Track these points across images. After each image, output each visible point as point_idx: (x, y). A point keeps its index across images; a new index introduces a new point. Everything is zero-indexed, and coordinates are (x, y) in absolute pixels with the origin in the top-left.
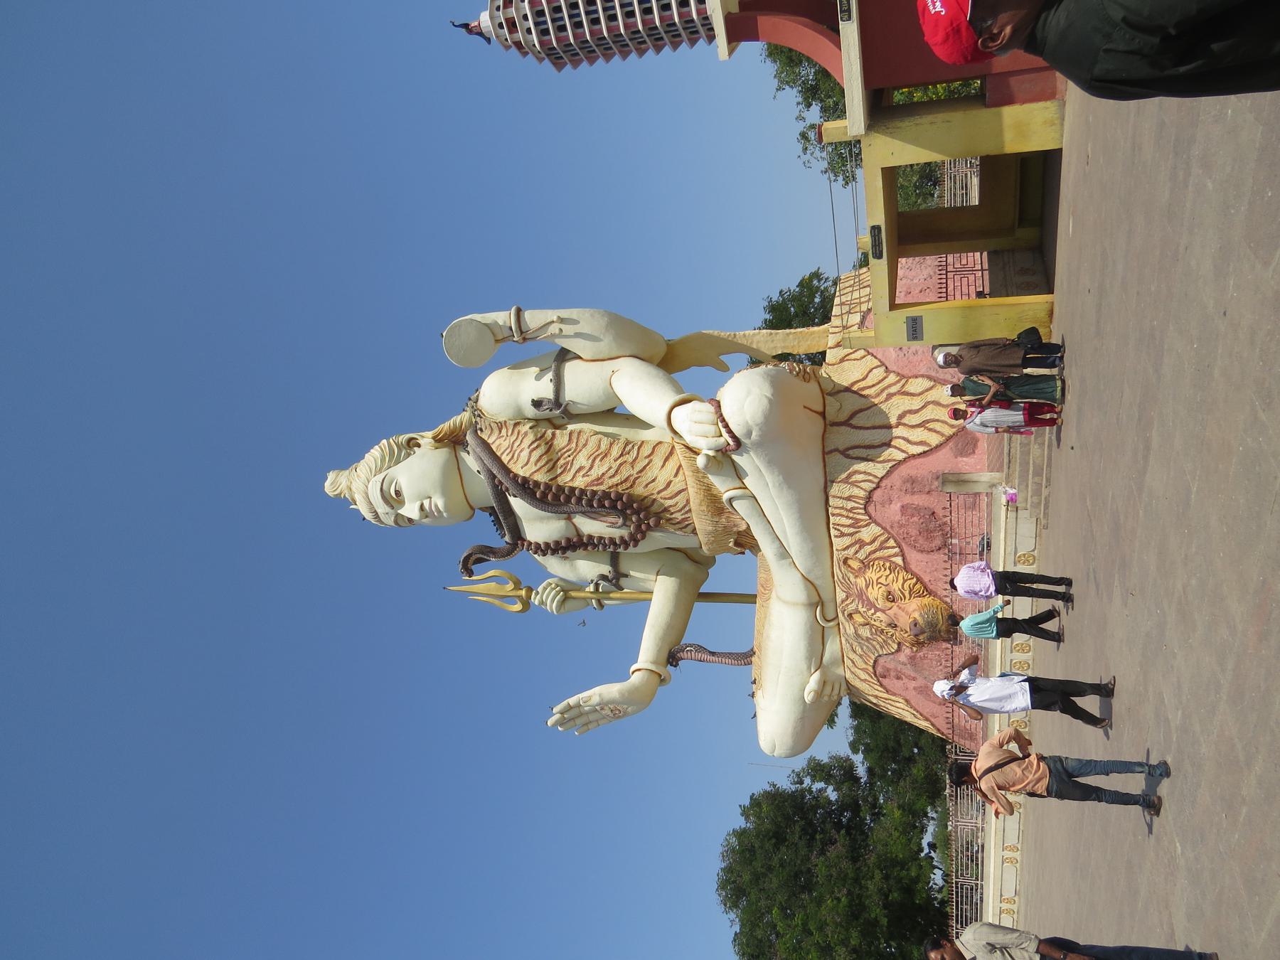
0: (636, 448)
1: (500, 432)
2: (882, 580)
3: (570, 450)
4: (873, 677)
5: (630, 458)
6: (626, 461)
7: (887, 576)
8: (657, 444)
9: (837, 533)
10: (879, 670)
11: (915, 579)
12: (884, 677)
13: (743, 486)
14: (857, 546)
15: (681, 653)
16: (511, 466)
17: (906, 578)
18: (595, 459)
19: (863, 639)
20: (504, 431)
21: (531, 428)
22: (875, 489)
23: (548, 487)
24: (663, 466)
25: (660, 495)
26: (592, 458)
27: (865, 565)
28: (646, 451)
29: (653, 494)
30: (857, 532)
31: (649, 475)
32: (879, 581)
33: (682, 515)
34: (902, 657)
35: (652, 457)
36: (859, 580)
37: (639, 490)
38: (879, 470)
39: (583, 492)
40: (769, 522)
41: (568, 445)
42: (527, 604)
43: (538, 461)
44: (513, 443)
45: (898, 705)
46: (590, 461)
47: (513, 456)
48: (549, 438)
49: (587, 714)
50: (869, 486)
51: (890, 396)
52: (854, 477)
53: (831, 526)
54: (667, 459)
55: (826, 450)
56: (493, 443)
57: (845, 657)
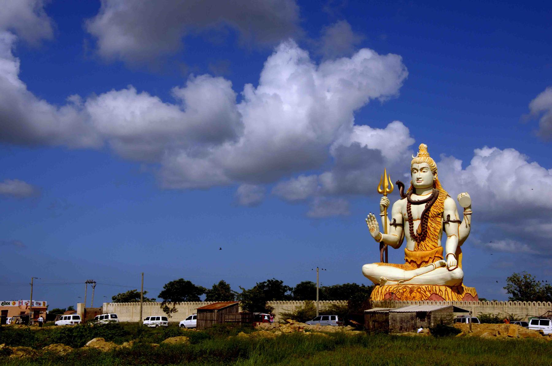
2: (417, 296)
5: (434, 237)
9: (426, 287)
12: (389, 294)
14: (424, 291)
16: (433, 206)
18: (434, 228)
20: (440, 204)
22: (439, 296)
23: (428, 216)
24: (433, 245)
25: (425, 244)
27: (420, 292)
28: (436, 241)
30: (427, 291)
31: (430, 241)
37: (427, 239)
38: (443, 297)
39: (427, 225)
41: (437, 221)
42: (382, 194)
45: (381, 297)
46: (434, 227)
50: (440, 294)
51: (458, 299)
54: (434, 246)
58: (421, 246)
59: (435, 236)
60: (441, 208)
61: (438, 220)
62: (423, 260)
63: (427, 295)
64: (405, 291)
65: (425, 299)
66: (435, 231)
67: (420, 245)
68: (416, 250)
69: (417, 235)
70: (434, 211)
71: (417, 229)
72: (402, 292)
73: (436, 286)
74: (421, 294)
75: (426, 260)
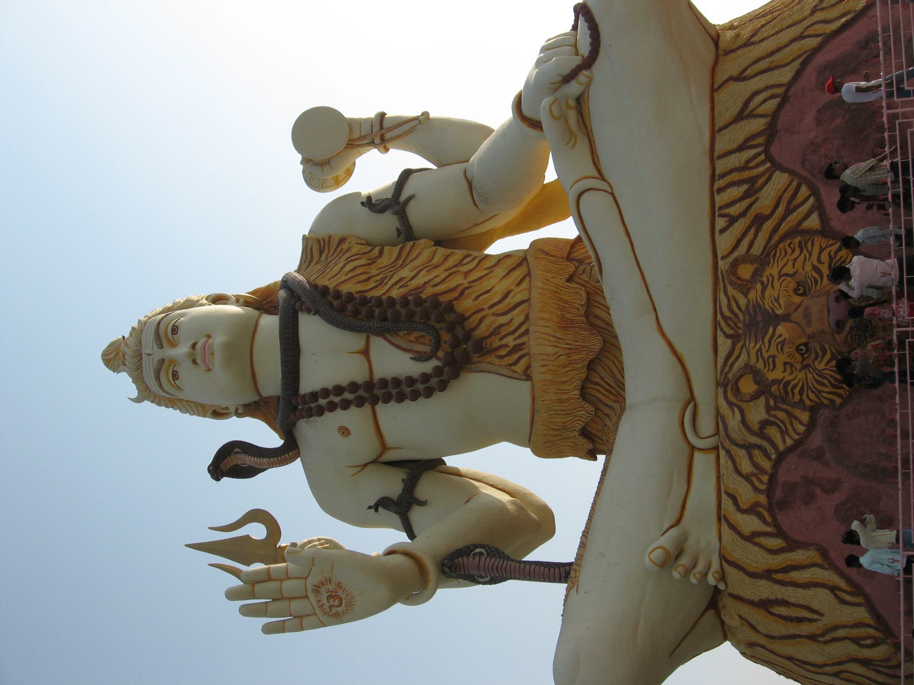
2: (789, 269)
3: (393, 267)
4: (766, 514)
6: (458, 271)
7: (795, 260)
10: (778, 494)
11: (839, 244)
12: (783, 505)
14: (752, 231)
15: (465, 558)
17: (823, 246)
19: (753, 433)
22: (780, 107)
25: (494, 310)
27: (763, 261)
29: (483, 310)
31: (485, 285)
32: (782, 272)
33: (516, 339)
34: (817, 440)
35: (493, 269)
36: (752, 295)
37: (466, 305)
38: (785, 75)
40: (628, 234)
41: (394, 262)
46: (415, 272)
49: (290, 599)
50: (772, 104)
52: (751, 104)
53: (717, 213)
55: (716, 86)
57: (724, 496)
58: (504, 331)
59: (466, 264)
60: (339, 249)
63: (777, 206)
64: (757, 376)
65: (812, 200)
68: (524, 361)
69: (440, 354)
71: (411, 355)
72: (762, 399)
73: (716, 154)
74: (776, 246)
75: (577, 296)
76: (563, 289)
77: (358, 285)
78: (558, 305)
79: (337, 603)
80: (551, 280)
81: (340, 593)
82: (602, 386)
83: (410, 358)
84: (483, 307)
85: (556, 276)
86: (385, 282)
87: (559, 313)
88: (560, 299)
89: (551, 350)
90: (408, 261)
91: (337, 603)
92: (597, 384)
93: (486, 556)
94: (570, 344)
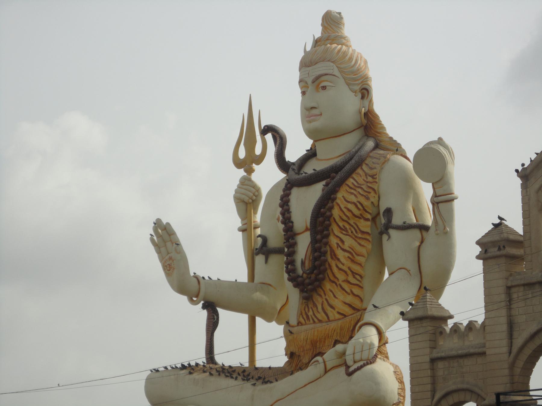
0: (358, 283)
1: (370, 176)
6: (348, 275)
8: (360, 298)
13: (327, 370)
16: (344, 188)
20: (370, 179)
21: (372, 203)
25: (325, 302)
26: (351, 250)
28: (356, 291)
33: (311, 316)
35: (351, 295)
37: (328, 286)
39: (326, 244)
43: (349, 210)
44: (362, 188)
46: (348, 249)
47: (351, 188)
48: (365, 216)
49: (166, 246)
54: (350, 305)
56: (362, 169)
58: (315, 309)
59: (354, 277)
60: (370, 190)
61: (363, 229)
62: (318, 352)
66: (353, 261)
67: (310, 305)
70: (348, 202)
71: (304, 258)
76: (331, 340)
77: (338, 217)
78: (322, 338)
79: (168, 269)
80: (335, 332)
81: (171, 270)
82: (297, 362)
83: (302, 259)
84: (327, 295)
85: (338, 334)
86: (344, 232)
87: (318, 339)
88: (325, 339)
89: (302, 337)
90: (358, 241)
91: (168, 269)
92: (298, 360)
93: (213, 321)
94: (305, 347)
